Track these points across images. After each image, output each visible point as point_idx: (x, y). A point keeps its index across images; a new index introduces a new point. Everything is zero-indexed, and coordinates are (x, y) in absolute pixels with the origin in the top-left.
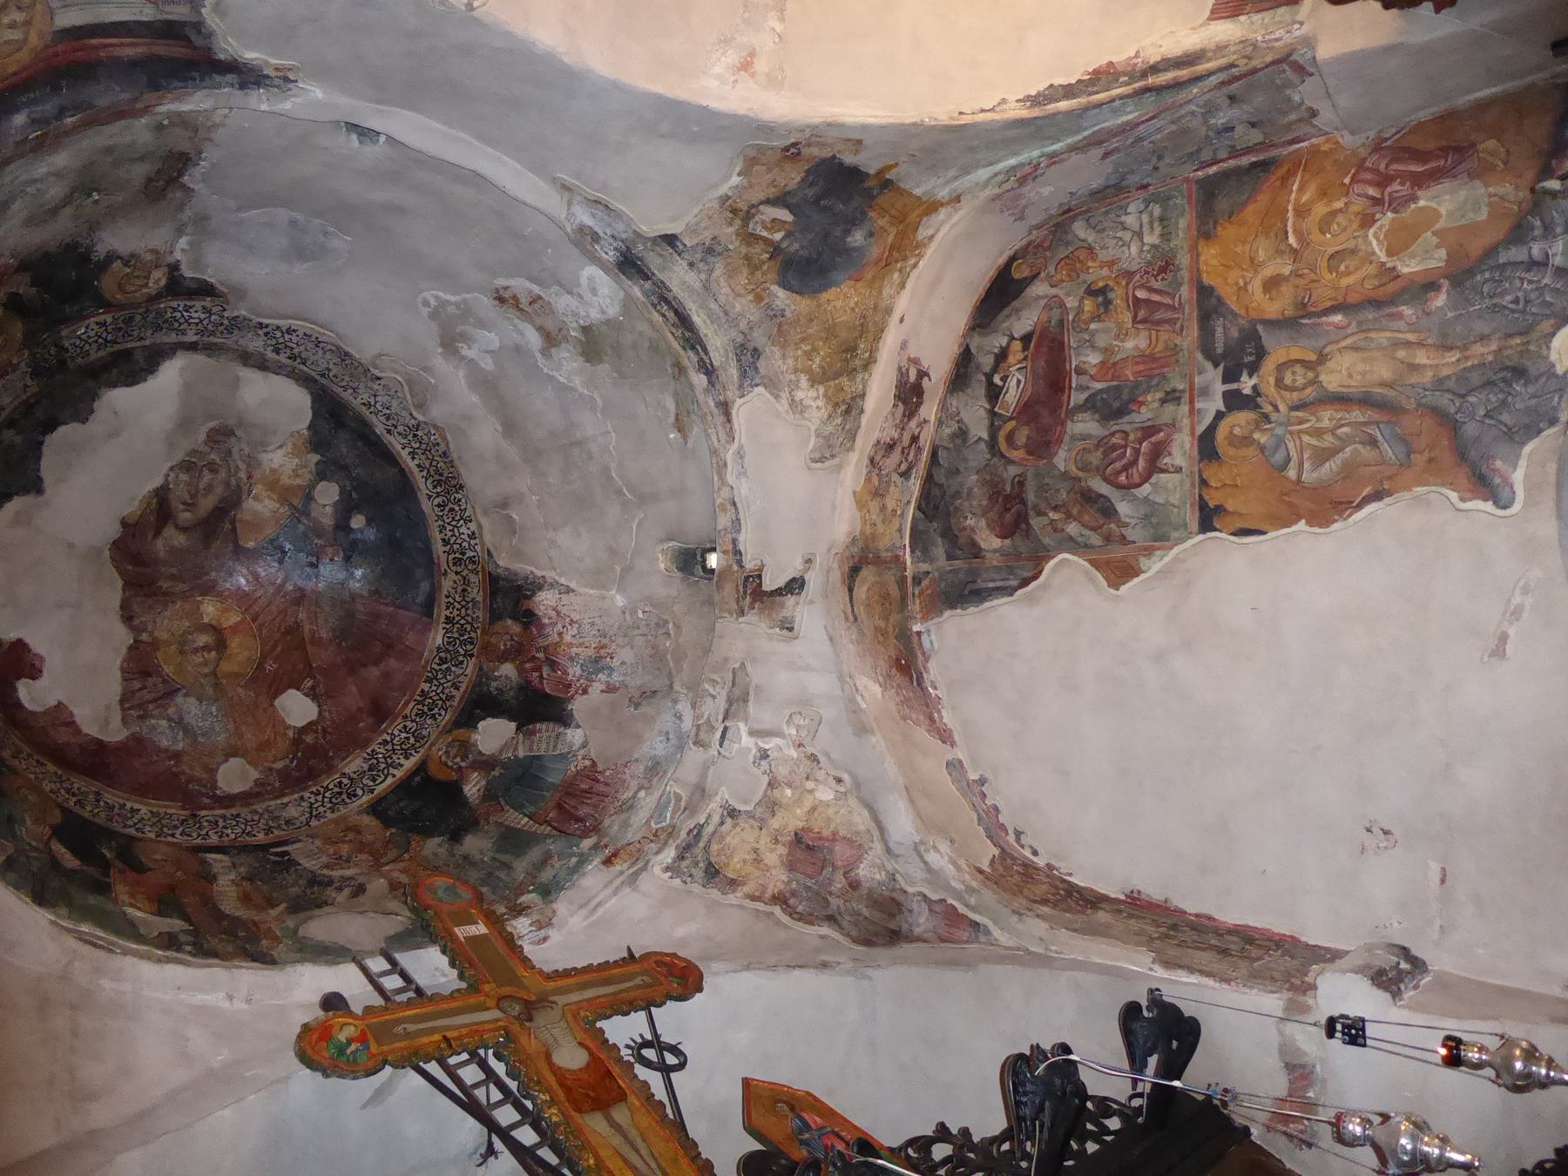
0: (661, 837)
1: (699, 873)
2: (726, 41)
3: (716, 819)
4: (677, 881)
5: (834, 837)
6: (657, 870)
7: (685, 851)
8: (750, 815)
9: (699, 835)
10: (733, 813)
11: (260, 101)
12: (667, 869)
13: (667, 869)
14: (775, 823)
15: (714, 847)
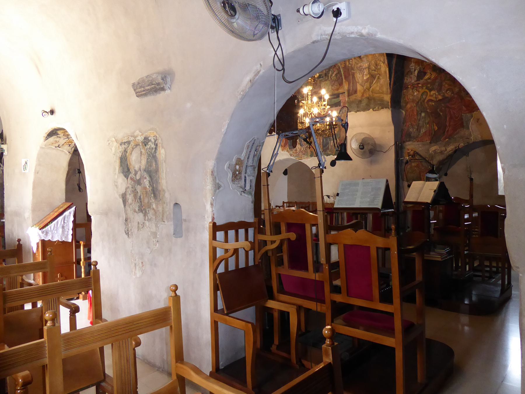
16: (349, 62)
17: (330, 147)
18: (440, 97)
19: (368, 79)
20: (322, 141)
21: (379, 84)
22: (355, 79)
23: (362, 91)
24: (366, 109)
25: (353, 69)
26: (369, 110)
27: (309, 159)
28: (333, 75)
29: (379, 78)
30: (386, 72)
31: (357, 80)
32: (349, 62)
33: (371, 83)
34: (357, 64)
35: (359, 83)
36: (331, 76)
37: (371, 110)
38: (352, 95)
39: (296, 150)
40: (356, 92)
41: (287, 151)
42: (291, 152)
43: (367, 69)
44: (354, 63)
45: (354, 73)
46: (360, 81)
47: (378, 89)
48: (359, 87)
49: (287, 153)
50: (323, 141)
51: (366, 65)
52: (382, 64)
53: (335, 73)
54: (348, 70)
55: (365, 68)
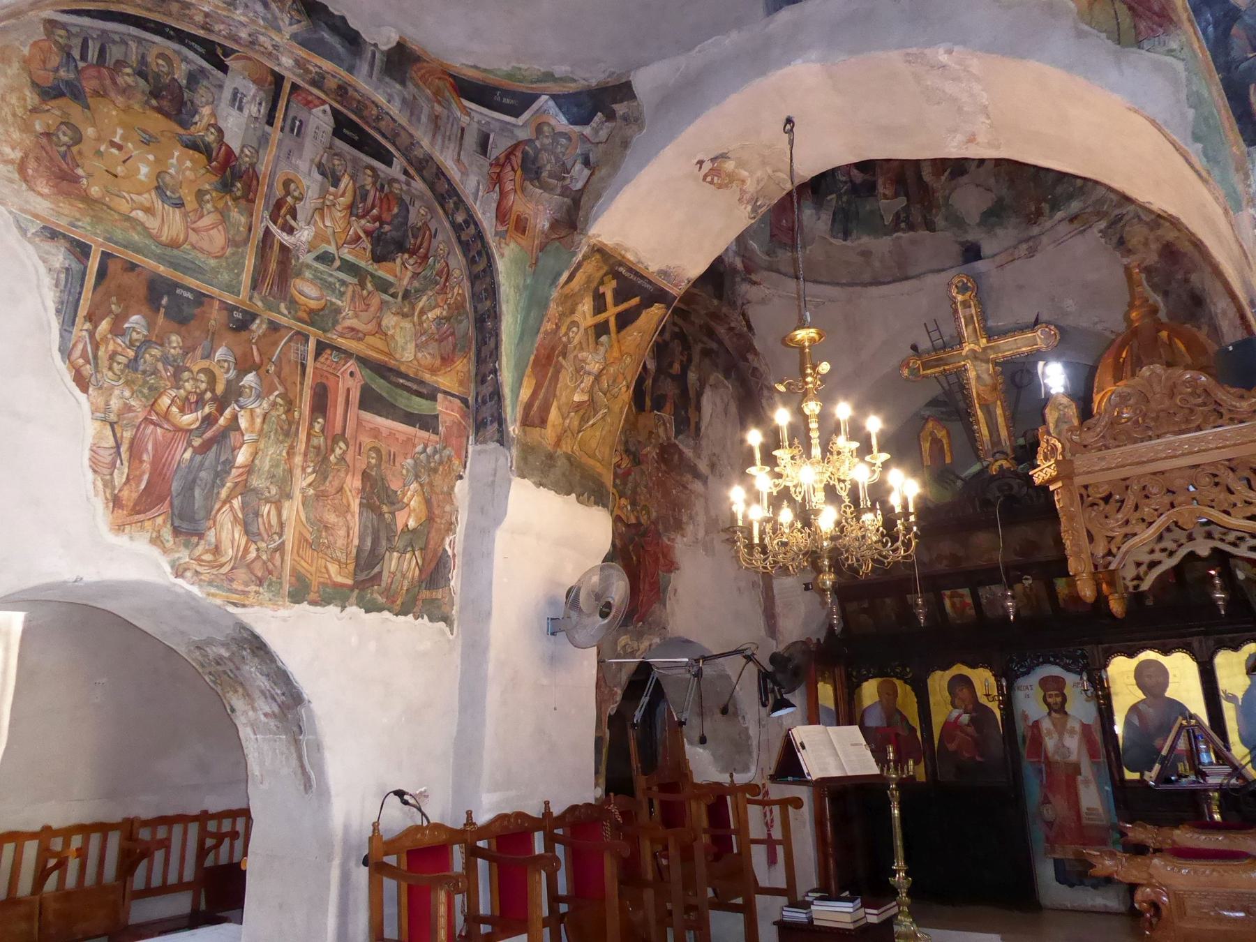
0: (1100, 215)
1: (1115, 240)
2: (954, 130)
3: (1131, 215)
4: (1103, 240)
5: (1185, 254)
6: (1095, 230)
7: (1112, 224)
8: (1147, 223)
9: (1121, 219)
10: (1139, 217)
11: (755, 288)
12: (1101, 231)
13: (1101, 231)
14: (1159, 232)
15: (1127, 229)
16: (569, 329)
17: (385, 577)
18: (633, 521)
19: (580, 404)
20: (356, 542)
21: (598, 434)
22: (556, 384)
23: (559, 430)
24: (564, 488)
25: (564, 355)
26: (568, 494)
27: (283, 612)
28: (431, 315)
29: (603, 418)
30: (621, 412)
31: (558, 393)
32: (569, 329)
33: (584, 420)
34: (582, 349)
35: (558, 401)
36: (422, 312)
37: (573, 495)
38: (533, 425)
39: (217, 550)
40: (543, 422)
41: (157, 541)
42: (184, 556)
43: (592, 378)
44: (577, 339)
45: (562, 366)
46: (563, 399)
47: (593, 444)
48: (554, 414)
49: (155, 552)
50: (362, 538)
51: (594, 367)
52: (624, 389)
53: (437, 311)
54: (553, 349)
55: (589, 373)
